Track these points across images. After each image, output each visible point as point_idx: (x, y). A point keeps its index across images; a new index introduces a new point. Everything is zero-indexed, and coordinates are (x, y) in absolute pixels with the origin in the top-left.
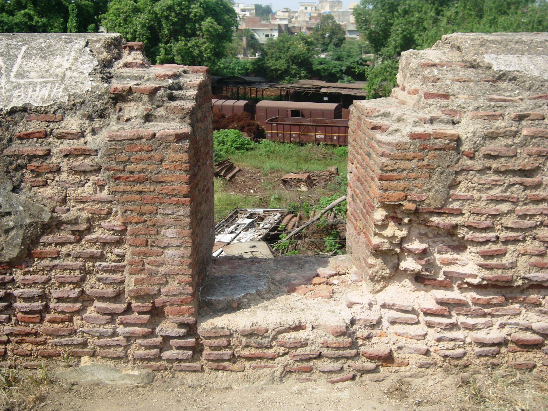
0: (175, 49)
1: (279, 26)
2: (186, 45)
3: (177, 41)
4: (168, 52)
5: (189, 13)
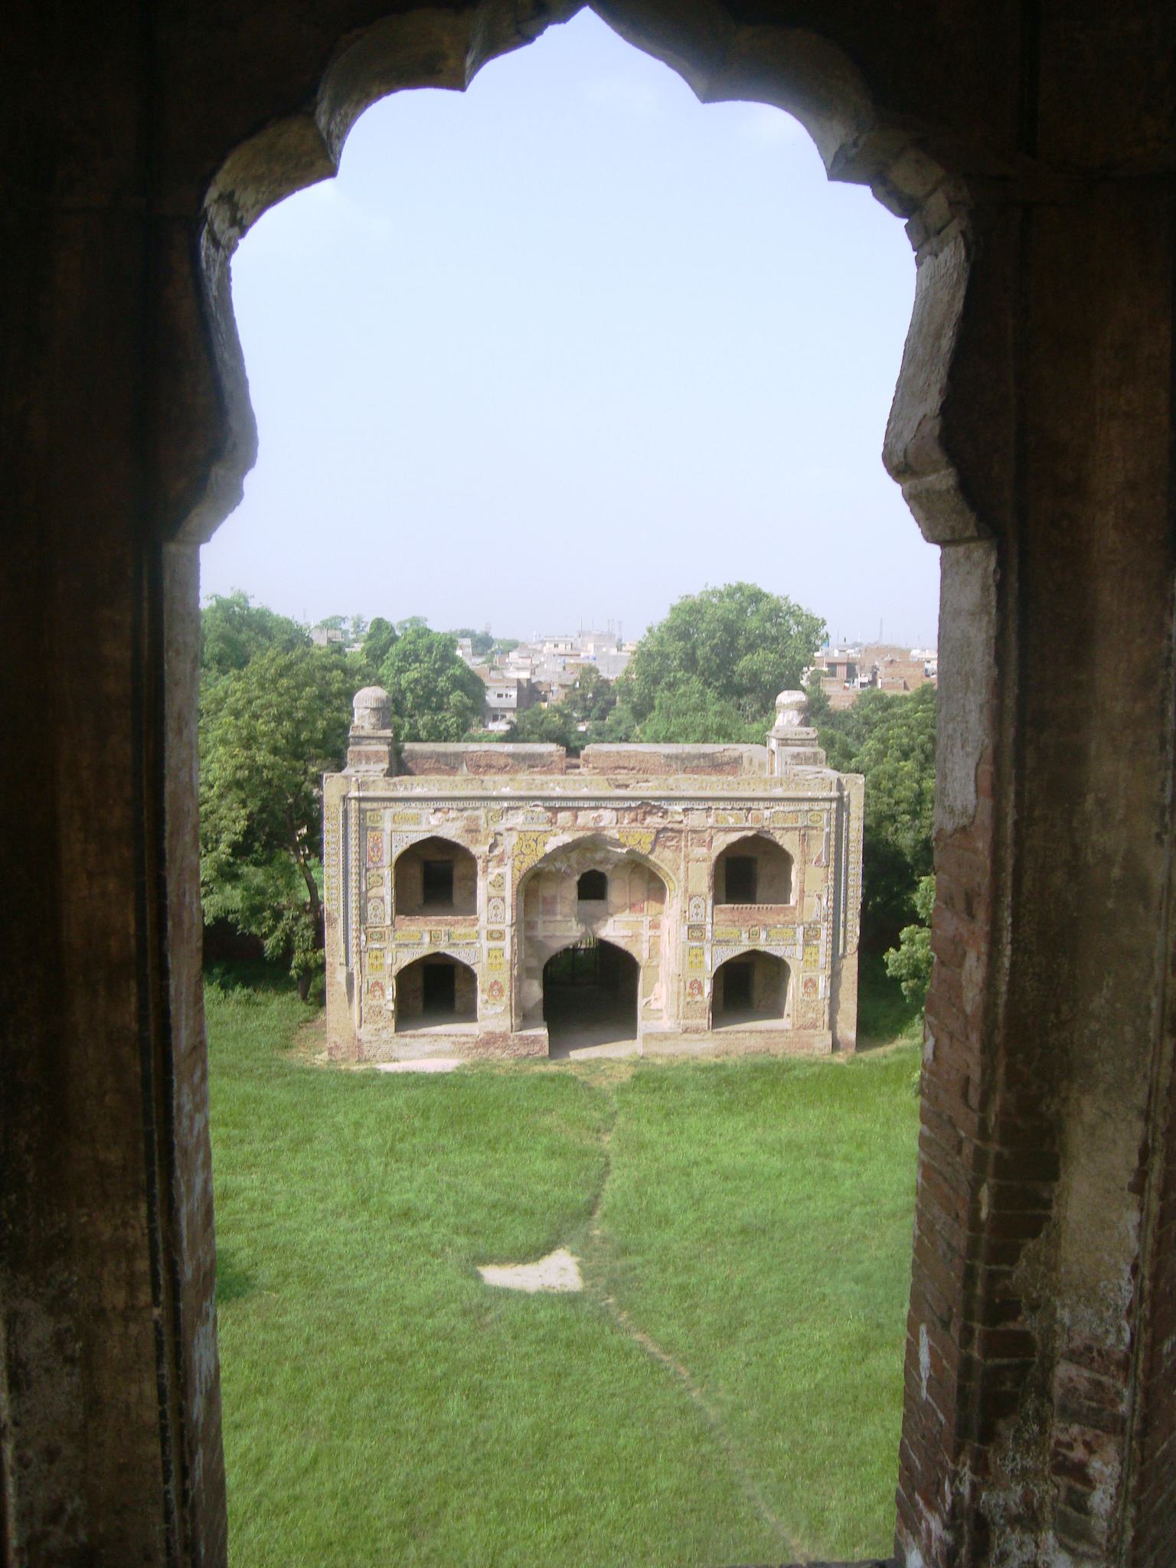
0: (421, 723)
1: (519, 681)
2: (433, 719)
3: (423, 715)
4: (413, 727)
5: (436, 687)
